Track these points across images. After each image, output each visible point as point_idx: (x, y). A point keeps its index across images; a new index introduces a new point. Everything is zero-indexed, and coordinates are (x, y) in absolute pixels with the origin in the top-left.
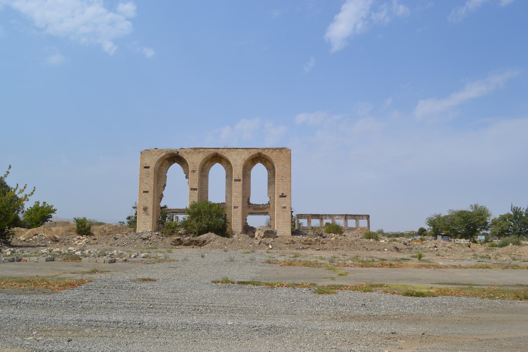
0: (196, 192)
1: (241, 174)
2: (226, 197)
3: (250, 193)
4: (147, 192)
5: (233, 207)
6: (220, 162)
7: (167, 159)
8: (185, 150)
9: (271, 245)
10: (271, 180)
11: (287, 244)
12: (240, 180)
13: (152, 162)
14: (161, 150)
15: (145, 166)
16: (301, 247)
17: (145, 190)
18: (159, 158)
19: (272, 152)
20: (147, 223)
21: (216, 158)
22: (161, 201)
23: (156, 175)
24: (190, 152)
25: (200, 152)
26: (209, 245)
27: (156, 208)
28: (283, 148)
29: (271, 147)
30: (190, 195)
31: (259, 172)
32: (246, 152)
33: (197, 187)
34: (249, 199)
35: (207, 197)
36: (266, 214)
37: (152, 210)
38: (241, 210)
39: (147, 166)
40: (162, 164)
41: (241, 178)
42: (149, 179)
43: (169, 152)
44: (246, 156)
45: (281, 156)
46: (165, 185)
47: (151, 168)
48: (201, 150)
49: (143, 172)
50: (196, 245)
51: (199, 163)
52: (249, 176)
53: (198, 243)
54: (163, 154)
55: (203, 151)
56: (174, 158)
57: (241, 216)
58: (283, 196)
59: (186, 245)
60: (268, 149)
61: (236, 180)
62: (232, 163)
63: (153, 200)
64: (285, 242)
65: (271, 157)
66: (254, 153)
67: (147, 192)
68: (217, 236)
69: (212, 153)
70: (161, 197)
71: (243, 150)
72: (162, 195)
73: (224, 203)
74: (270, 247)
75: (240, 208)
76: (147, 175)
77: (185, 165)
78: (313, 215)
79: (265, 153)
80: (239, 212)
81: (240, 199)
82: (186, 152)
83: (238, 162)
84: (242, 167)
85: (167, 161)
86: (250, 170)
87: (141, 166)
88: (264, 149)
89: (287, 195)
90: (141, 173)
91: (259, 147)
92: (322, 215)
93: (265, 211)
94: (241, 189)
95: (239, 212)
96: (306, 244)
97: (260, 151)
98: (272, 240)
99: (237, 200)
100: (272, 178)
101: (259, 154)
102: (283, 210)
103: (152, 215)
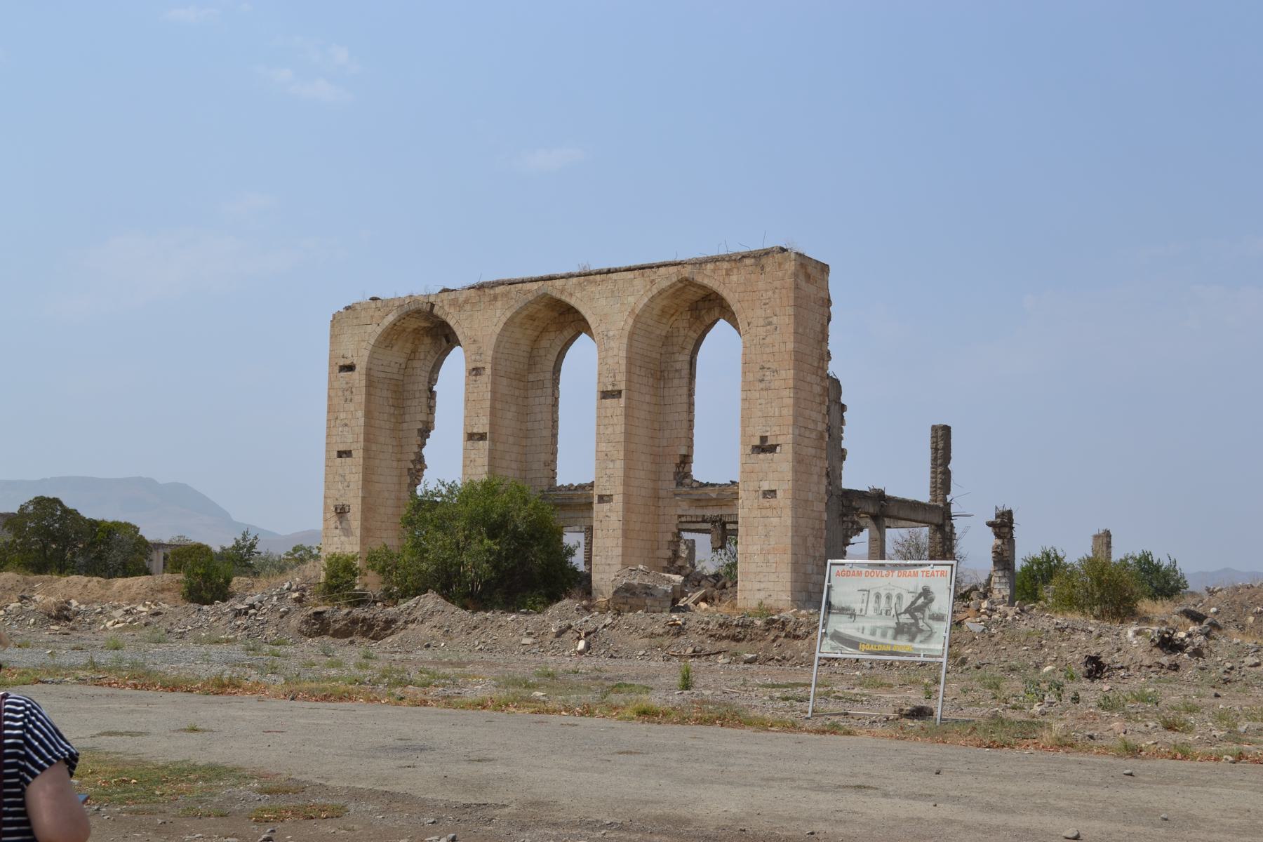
0: (484, 445)
1: (623, 368)
5: (596, 500)
12: (620, 392)
17: (342, 448)
18: (379, 330)
19: (728, 273)
24: (466, 301)
25: (495, 298)
28: (767, 253)
29: (723, 252)
30: (465, 458)
32: (639, 282)
37: (359, 515)
39: (348, 362)
40: (414, 352)
41: (622, 386)
42: (351, 407)
45: (761, 285)
50: (364, 634)
53: (371, 627)
54: (391, 318)
56: (427, 330)
59: (338, 634)
60: (715, 260)
64: (650, 630)
65: (725, 293)
71: (629, 275)
79: (710, 279)
80: (614, 517)
85: (427, 340)
88: (700, 263)
96: (721, 638)
97: (686, 272)
98: (609, 621)
102: (765, 502)
103: (358, 532)
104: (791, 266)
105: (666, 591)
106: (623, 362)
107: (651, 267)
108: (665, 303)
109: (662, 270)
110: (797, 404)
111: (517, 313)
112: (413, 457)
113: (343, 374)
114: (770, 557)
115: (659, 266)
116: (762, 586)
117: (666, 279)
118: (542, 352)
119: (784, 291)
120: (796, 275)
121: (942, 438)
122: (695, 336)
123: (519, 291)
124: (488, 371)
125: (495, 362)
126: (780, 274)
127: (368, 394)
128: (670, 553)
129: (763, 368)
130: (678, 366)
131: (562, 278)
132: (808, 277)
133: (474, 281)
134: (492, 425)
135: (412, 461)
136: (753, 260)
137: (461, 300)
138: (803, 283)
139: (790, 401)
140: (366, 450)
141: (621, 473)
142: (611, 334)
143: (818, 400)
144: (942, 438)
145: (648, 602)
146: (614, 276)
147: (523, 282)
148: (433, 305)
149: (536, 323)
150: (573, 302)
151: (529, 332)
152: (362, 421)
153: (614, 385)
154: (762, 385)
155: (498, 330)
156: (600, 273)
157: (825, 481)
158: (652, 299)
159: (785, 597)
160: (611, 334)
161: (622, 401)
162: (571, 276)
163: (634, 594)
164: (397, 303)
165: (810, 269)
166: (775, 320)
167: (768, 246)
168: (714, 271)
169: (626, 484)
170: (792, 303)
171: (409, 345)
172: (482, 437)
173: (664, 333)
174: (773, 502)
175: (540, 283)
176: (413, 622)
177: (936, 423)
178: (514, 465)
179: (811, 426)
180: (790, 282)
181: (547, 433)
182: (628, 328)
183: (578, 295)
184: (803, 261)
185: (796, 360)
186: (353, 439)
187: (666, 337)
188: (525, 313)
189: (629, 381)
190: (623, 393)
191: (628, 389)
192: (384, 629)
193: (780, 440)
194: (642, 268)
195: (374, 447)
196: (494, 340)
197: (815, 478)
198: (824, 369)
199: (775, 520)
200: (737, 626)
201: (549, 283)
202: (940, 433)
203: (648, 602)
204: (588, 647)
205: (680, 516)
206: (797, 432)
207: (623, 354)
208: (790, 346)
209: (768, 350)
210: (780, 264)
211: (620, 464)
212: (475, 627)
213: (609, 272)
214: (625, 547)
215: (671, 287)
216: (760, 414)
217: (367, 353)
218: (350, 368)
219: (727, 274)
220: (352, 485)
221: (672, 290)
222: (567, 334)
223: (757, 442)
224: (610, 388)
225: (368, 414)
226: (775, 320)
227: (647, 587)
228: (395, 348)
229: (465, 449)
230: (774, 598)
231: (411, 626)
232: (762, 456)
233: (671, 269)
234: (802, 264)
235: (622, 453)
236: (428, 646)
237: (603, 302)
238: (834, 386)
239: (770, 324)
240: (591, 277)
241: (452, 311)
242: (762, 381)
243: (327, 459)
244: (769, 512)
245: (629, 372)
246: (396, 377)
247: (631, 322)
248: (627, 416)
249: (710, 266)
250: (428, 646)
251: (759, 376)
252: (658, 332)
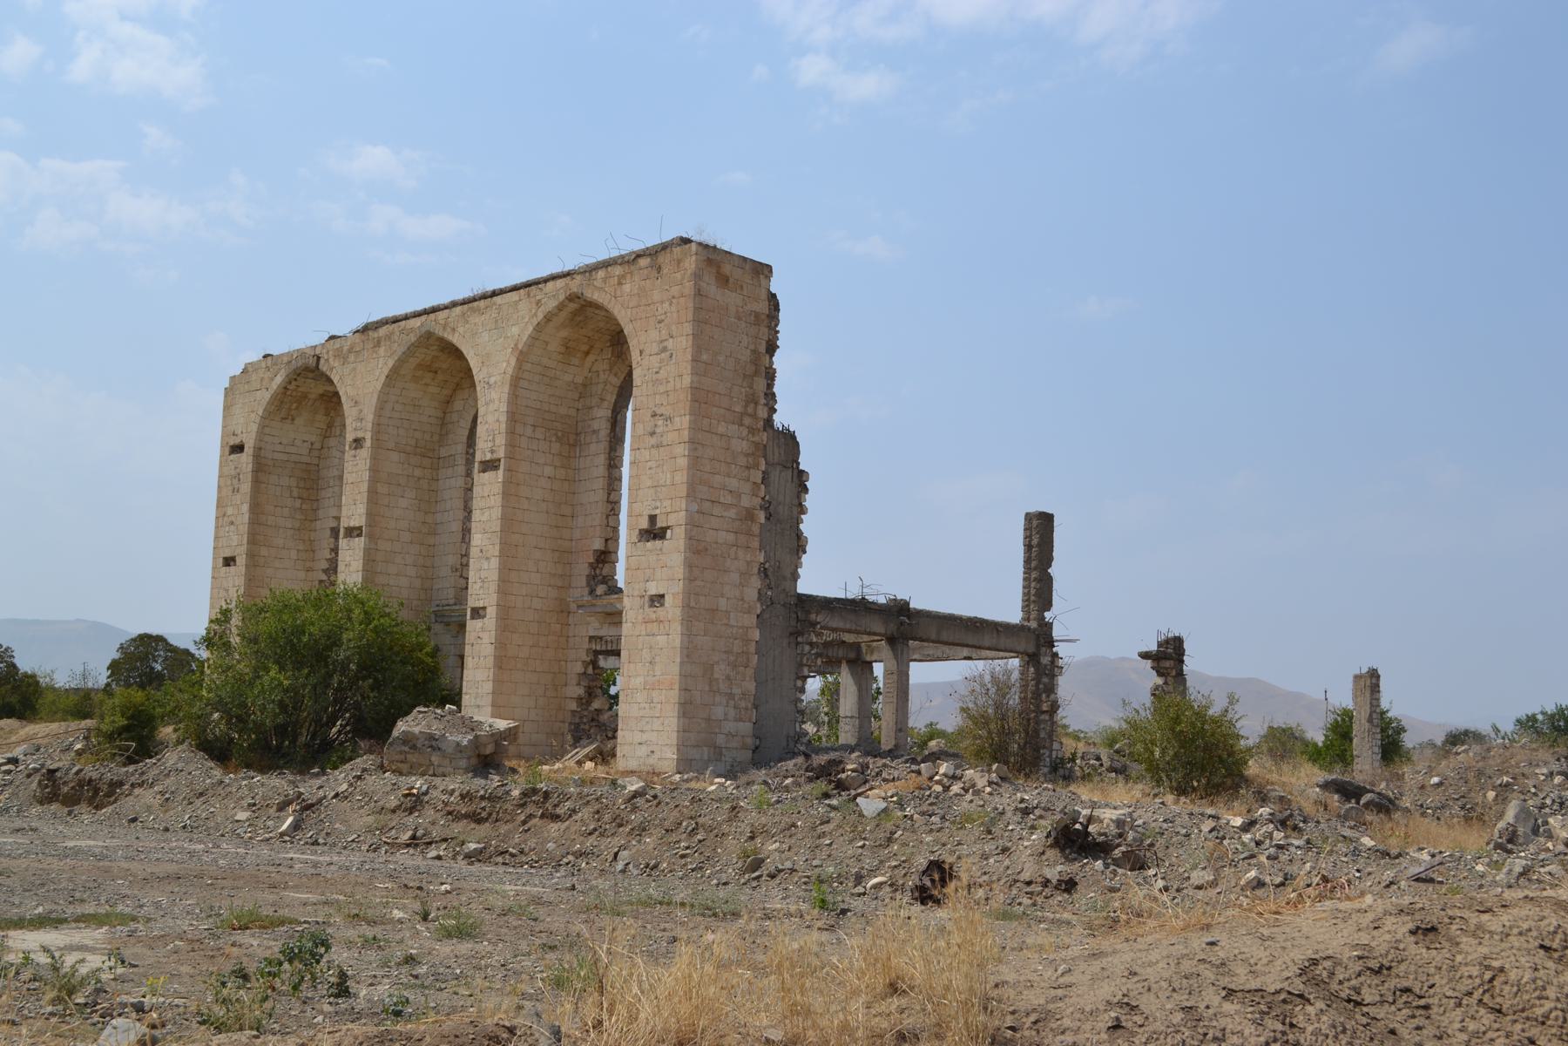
17: (228, 555)
18: (267, 396)
25: (378, 344)
28: (664, 247)
29: (615, 254)
41: (501, 454)
42: (238, 498)
43: (294, 365)
45: (656, 296)
48: (383, 331)
53: (96, 791)
54: (279, 379)
55: (389, 337)
71: (514, 296)
97: (575, 285)
102: (651, 613)
104: (690, 264)
105: (458, 744)
106: (503, 418)
107: (536, 283)
108: (564, 333)
109: (550, 284)
110: (695, 462)
111: (401, 362)
112: (325, 565)
114: (655, 694)
115: (546, 280)
116: (645, 737)
117: (552, 297)
118: (455, 417)
120: (697, 276)
121: (1040, 529)
122: (617, 381)
124: (368, 443)
125: (378, 428)
126: (678, 275)
127: (256, 482)
128: (581, 691)
129: (654, 415)
130: (596, 425)
131: (446, 307)
132: (723, 280)
133: (359, 323)
134: (370, 515)
135: (325, 571)
138: (711, 288)
139: (683, 462)
140: (251, 555)
141: (494, 576)
142: (492, 380)
143: (742, 461)
144: (1040, 529)
145: (435, 759)
147: (406, 317)
149: (440, 377)
150: (455, 339)
151: (432, 389)
153: (492, 452)
154: (653, 441)
155: (379, 386)
157: (756, 582)
158: (539, 328)
159: (669, 755)
160: (492, 380)
161: (501, 472)
162: (454, 304)
163: (414, 747)
164: (285, 359)
165: (727, 269)
166: (670, 344)
167: (666, 238)
168: (605, 280)
169: (503, 591)
170: (690, 317)
171: (320, 417)
173: (579, 380)
175: (424, 318)
176: (141, 785)
177: (1032, 510)
178: (411, 571)
179: (729, 499)
180: (689, 287)
181: (456, 527)
182: (510, 371)
184: (714, 260)
185: (694, 400)
186: (237, 544)
187: (585, 385)
188: (413, 362)
189: (511, 445)
191: (509, 457)
192: (108, 795)
193: (671, 520)
195: (264, 551)
196: (374, 400)
197: (735, 577)
198: (769, 422)
199: (661, 639)
200: (482, 798)
201: (432, 316)
202: (1035, 523)
203: (435, 759)
204: (296, 826)
205: (591, 638)
206: (695, 507)
207: (504, 408)
208: (687, 380)
209: (662, 389)
211: (495, 563)
212: (201, 794)
213: (494, 294)
214: (497, 682)
215: (561, 307)
216: (649, 483)
217: (254, 428)
218: (238, 449)
219: (620, 284)
221: (563, 315)
225: (256, 508)
227: (431, 737)
228: (299, 421)
230: (656, 756)
231: (137, 791)
233: (560, 283)
234: (709, 261)
236: (134, 820)
237: (486, 336)
238: (789, 441)
239: (665, 349)
242: (653, 434)
243: (214, 568)
244: (654, 627)
245: (511, 432)
246: (305, 459)
247: (513, 362)
248: (506, 494)
249: (601, 273)
250: (134, 820)
252: (568, 378)
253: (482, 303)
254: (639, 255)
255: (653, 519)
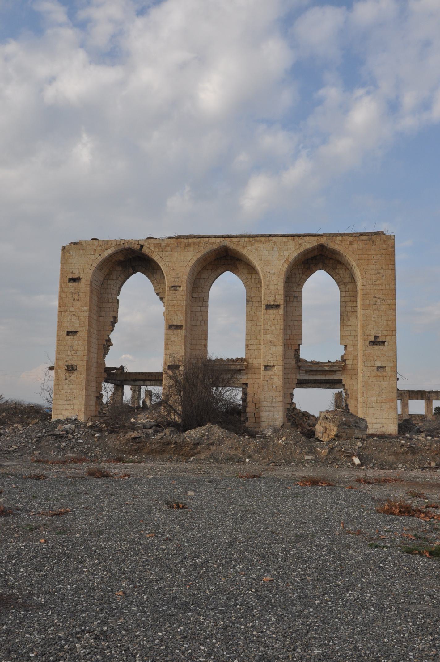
0: (182, 333)
1: (282, 292)
2: (247, 346)
3: (299, 336)
4: (74, 333)
5: (263, 368)
6: (234, 269)
7: (120, 263)
8: (156, 242)
9: (359, 456)
10: (349, 308)
11: (395, 454)
12: (278, 306)
13: (86, 267)
14: (106, 242)
15: (71, 276)
16: (433, 464)
18: (100, 259)
19: (351, 243)
20: (74, 402)
21: (224, 257)
22: (106, 353)
23: (95, 298)
24: (168, 245)
25: (189, 245)
26: (208, 454)
27: (94, 370)
31: (319, 287)
32: (291, 244)
33: (183, 323)
34: (298, 350)
35: (206, 346)
36: (337, 383)
38: (281, 373)
39: (76, 276)
41: (281, 302)
42: (78, 304)
43: (121, 247)
44: (292, 251)
46: (115, 320)
47: (83, 281)
48: (191, 240)
49: (66, 290)
51: (188, 269)
52: (298, 299)
54: (109, 252)
56: (132, 259)
57: (281, 388)
58: (376, 342)
59: (151, 452)
61: (268, 307)
62: (258, 268)
63: (89, 351)
64: (392, 450)
66: (309, 246)
67: (74, 333)
68: (226, 433)
69: (215, 247)
70: (106, 345)
71: (285, 239)
72: (109, 340)
73: (242, 360)
74: (357, 461)
75: (278, 370)
76: (76, 297)
77: (158, 277)
78: (413, 392)
80: (276, 379)
81: (279, 349)
82: (158, 246)
83: (272, 264)
84: (282, 278)
85: (119, 269)
86: (300, 285)
87: (62, 277)
88: (332, 236)
89: (388, 338)
90: (62, 291)
91: (321, 232)
92: (430, 392)
93: (335, 377)
94: (279, 327)
95: (276, 379)
97: (323, 241)
99: (273, 354)
100: (349, 304)
101: (321, 247)
102: (379, 374)
107: (299, 236)
109: (308, 238)
113: (71, 284)
114: (382, 404)
115: (304, 236)
116: (378, 421)
117: (310, 244)
119: (388, 256)
123: (207, 243)
131: (236, 237)
136: (367, 237)
137: (163, 244)
142: (272, 272)
146: (274, 239)
147: (209, 237)
148: (142, 247)
152: (87, 314)
154: (374, 307)
156: (264, 236)
162: (243, 236)
163: (349, 426)
164: (114, 243)
166: (382, 271)
168: (341, 241)
172: (178, 327)
174: (384, 373)
175: (222, 239)
176: (212, 444)
183: (249, 248)
190: (282, 307)
194: (293, 236)
199: (385, 384)
201: (228, 239)
209: (378, 288)
210: (384, 241)
213: (270, 236)
216: (374, 323)
220: (78, 354)
222: (219, 271)
223: (373, 339)
224: (272, 303)
226: (382, 271)
228: (103, 271)
229: (166, 334)
232: (376, 347)
235: (282, 341)
239: (379, 273)
240: (258, 239)
241: (156, 250)
242: (375, 304)
251: (372, 302)
253: (262, 239)
254: (361, 234)
255: (376, 337)
